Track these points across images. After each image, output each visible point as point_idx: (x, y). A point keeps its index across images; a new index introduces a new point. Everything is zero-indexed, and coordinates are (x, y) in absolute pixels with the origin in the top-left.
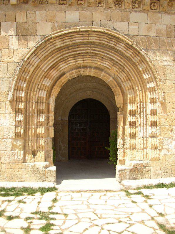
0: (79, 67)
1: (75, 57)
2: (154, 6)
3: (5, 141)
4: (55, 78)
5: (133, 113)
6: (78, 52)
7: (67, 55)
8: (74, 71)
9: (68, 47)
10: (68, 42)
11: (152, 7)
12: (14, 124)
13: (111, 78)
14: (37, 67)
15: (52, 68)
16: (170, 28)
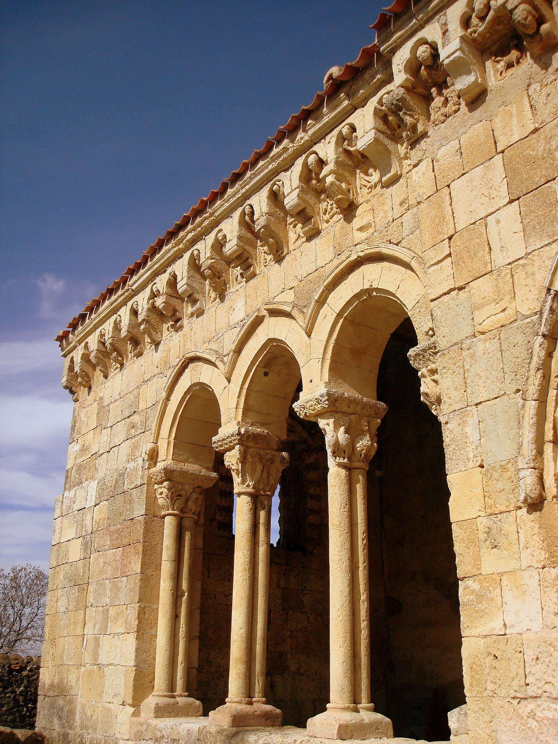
3: (532, 715)
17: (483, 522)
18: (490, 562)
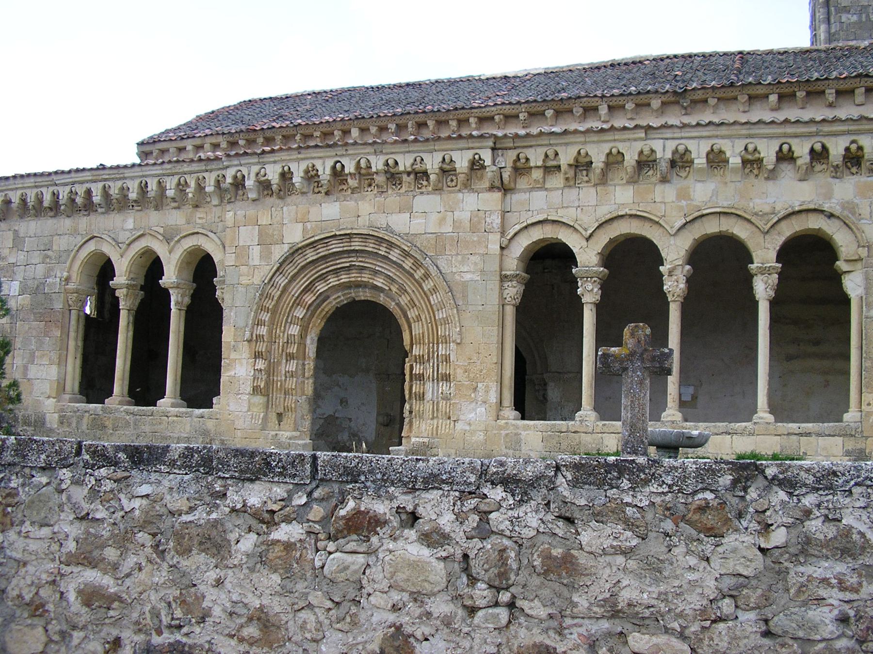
2: (452, 180)
5: (420, 360)
6: (339, 266)
12: (252, 373)
13: (393, 304)
15: (306, 290)
16: (477, 215)
17: (233, 343)
18: (233, 355)
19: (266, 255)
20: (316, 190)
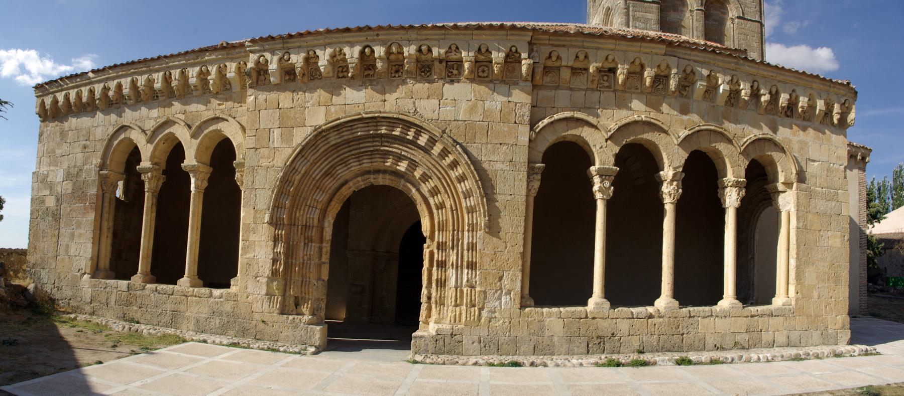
0: (368, 172)
1: (358, 157)
2: (483, 71)
4: (333, 188)
7: (346, 155)
8: (359, 179)
9: (348, 142)
10: (347, 135)
11: (480, 74)
14: (306, 173)
15: (327, 174)
19: (287, 138)
20: (341, 75)
